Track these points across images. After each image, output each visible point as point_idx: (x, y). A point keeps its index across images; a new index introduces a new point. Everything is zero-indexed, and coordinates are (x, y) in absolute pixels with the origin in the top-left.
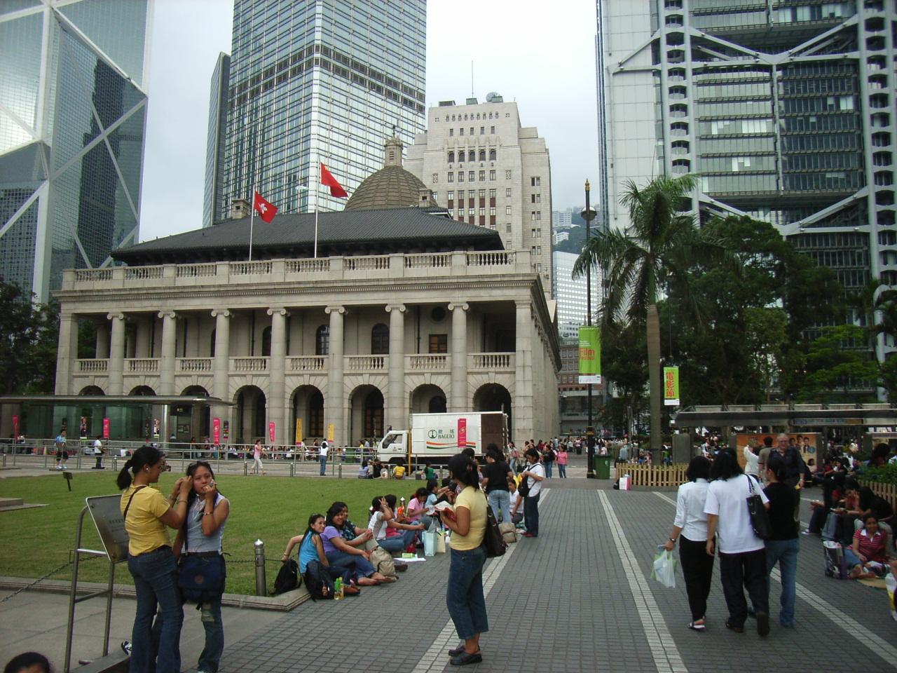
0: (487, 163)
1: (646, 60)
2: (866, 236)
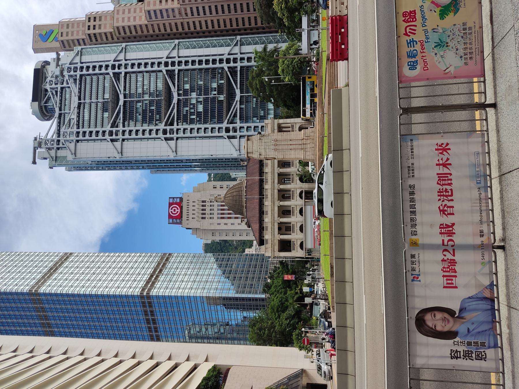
0: (207, 204)
1: (172, 143)
2: (241, 67)
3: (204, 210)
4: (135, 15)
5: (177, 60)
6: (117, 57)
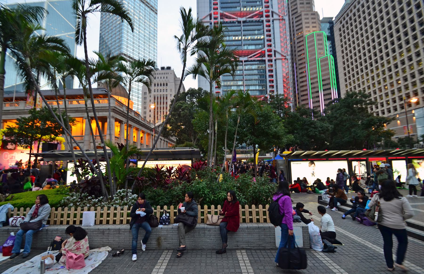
3: (161, 85)
5: (273, 58)
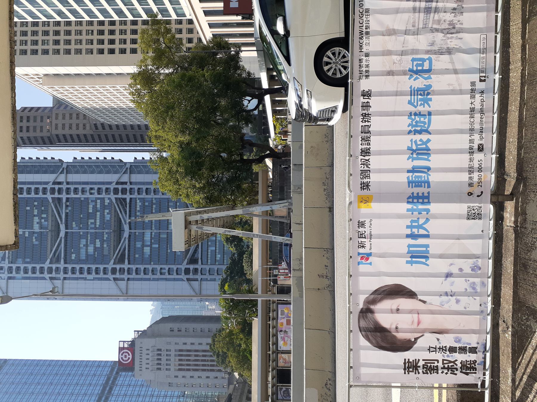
0: (162, 353)
3: (160, 359)
4: (77, 121)
5: (128, 187)
6: (56, 178)
